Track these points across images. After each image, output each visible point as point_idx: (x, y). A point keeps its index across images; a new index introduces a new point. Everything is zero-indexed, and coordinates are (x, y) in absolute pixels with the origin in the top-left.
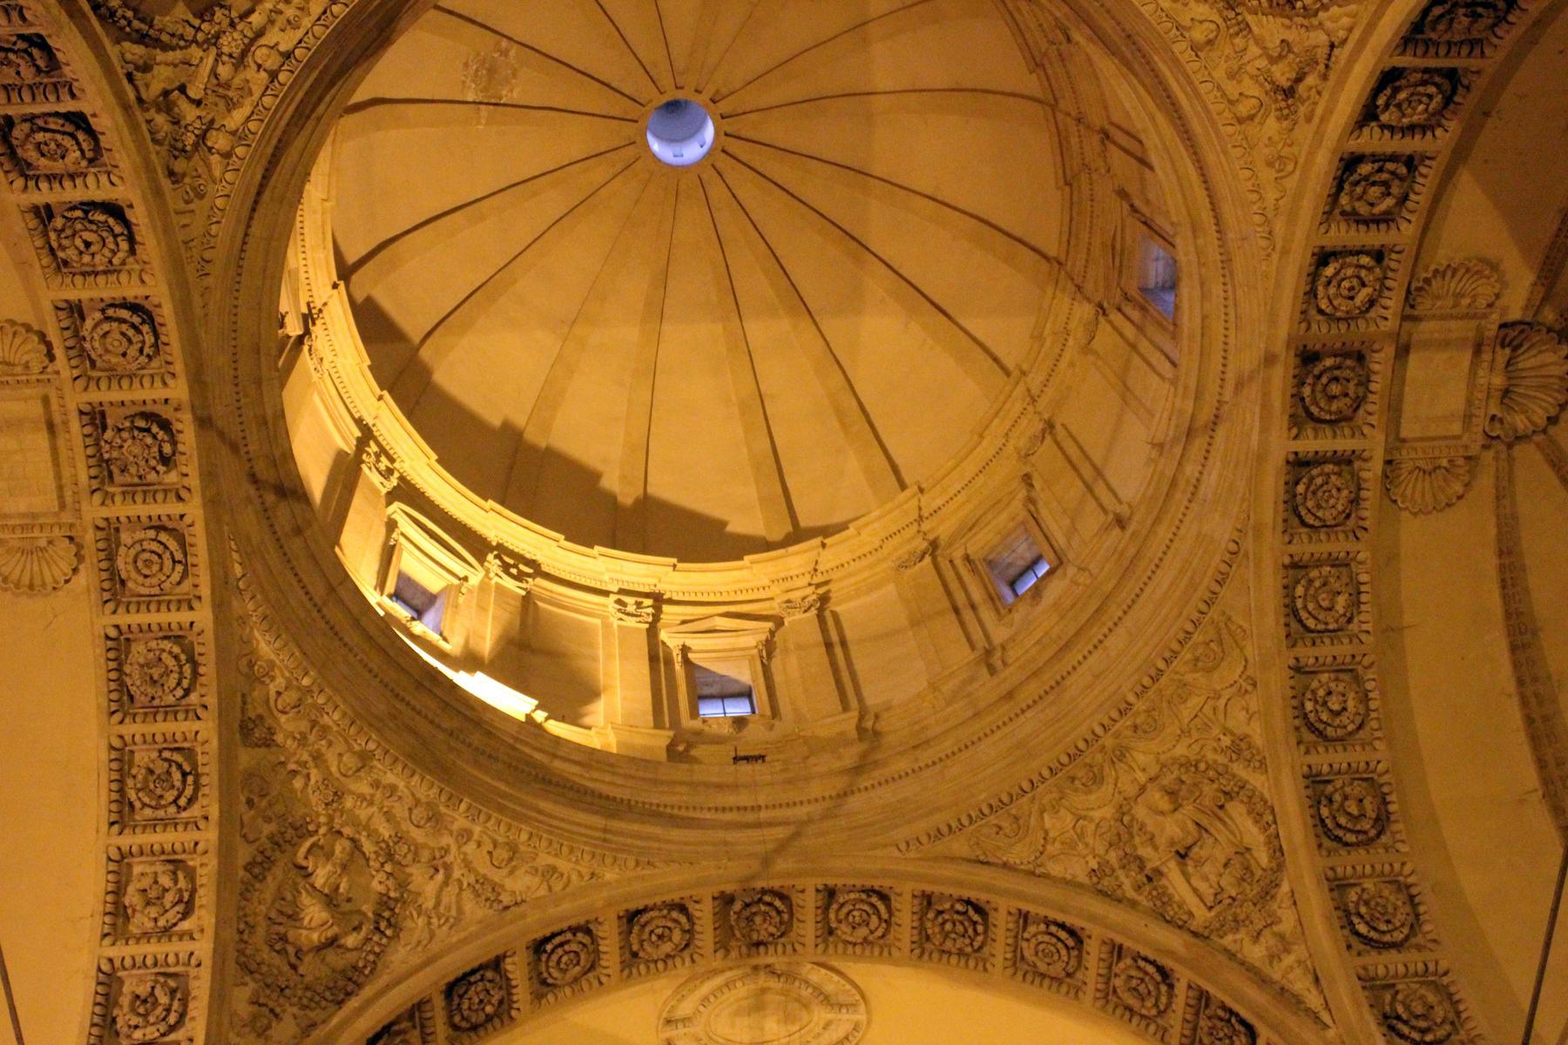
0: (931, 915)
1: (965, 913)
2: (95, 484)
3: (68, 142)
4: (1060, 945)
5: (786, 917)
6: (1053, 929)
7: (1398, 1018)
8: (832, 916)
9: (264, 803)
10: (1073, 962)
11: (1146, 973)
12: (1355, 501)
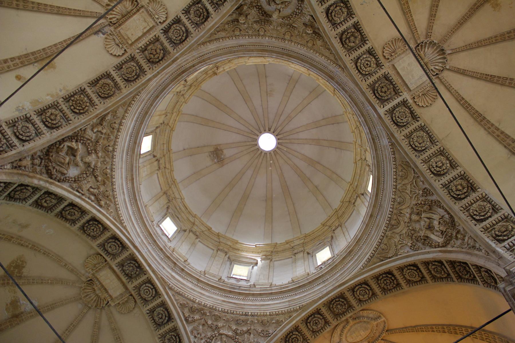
0: (379, 282)
1: (387, 276)
2: (128, 280)
3: (72, 210)
4: (413, 271)
5: (345, 302)
6: (409, 268)
7: (499, 236)
8: (356, 296)
9: (199, 336)
10: (420, 273)
11: (436, 265)
12: (412, 113)
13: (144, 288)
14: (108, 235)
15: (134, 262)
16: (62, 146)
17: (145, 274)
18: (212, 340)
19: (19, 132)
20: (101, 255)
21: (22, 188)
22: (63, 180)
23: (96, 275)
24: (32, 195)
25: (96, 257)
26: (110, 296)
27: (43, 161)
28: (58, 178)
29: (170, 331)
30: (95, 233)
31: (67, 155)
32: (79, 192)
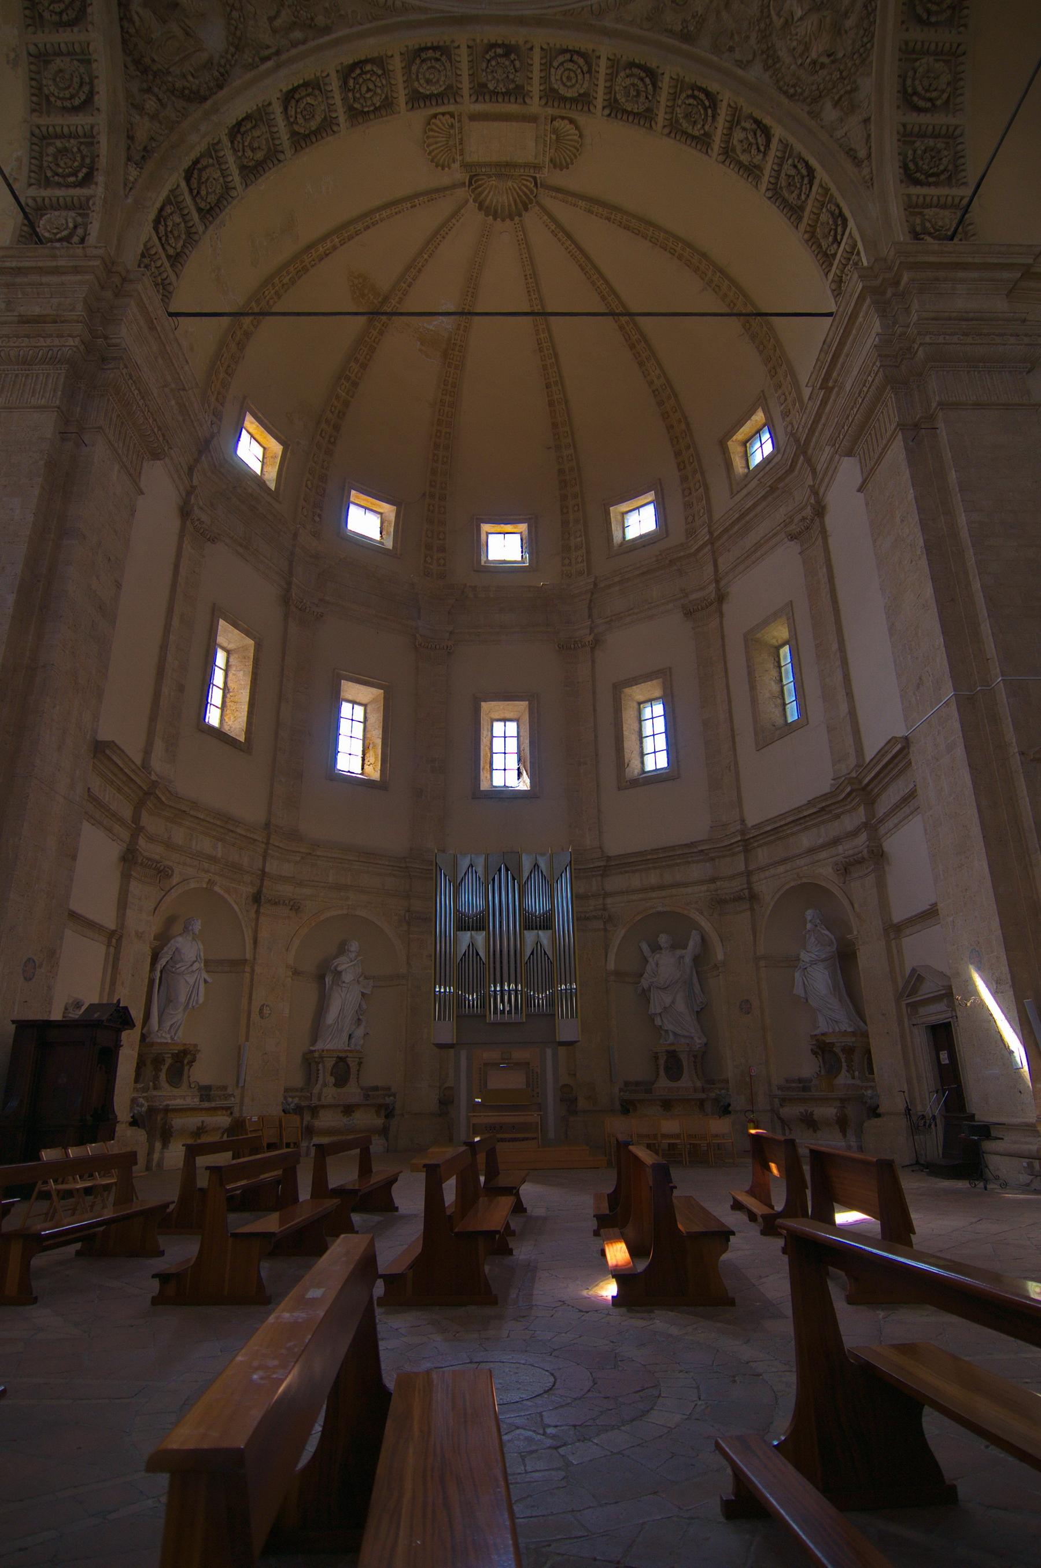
9: (736, 37)
13: (558, 77)
14: (397, 65)
15: (491, 53)
16: (136, 17)
17: (531, 49)
18: (769, 16)
19: (66, 99)
20: (435, 116)
21: (195, 175)
22: (222, 75)
23: (468, 159)
24: (224, 167)
25: (432, 130)
26: (526, 165)
27: (156, 90)
28: (212, 84)
29: (674, 97)
30: (379, 91)
31: (165, 22)
32: (268, 58)
